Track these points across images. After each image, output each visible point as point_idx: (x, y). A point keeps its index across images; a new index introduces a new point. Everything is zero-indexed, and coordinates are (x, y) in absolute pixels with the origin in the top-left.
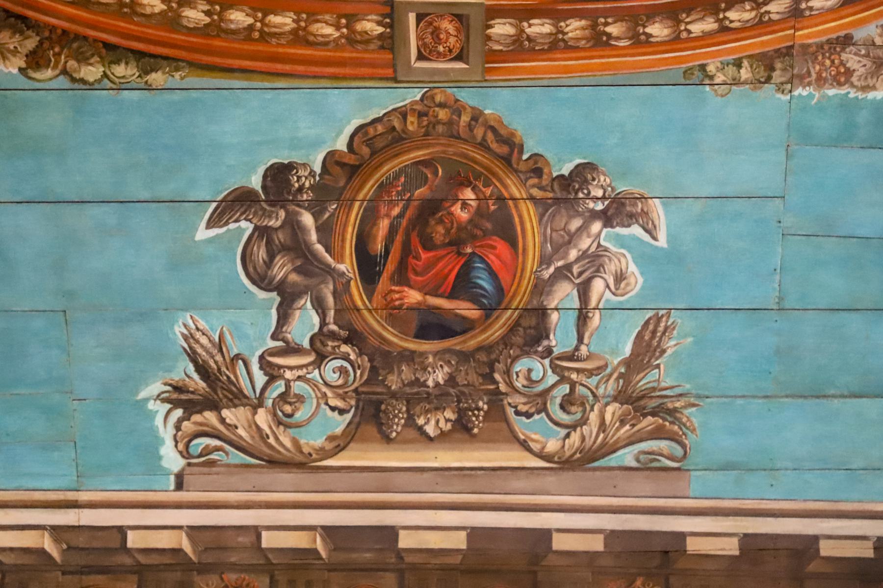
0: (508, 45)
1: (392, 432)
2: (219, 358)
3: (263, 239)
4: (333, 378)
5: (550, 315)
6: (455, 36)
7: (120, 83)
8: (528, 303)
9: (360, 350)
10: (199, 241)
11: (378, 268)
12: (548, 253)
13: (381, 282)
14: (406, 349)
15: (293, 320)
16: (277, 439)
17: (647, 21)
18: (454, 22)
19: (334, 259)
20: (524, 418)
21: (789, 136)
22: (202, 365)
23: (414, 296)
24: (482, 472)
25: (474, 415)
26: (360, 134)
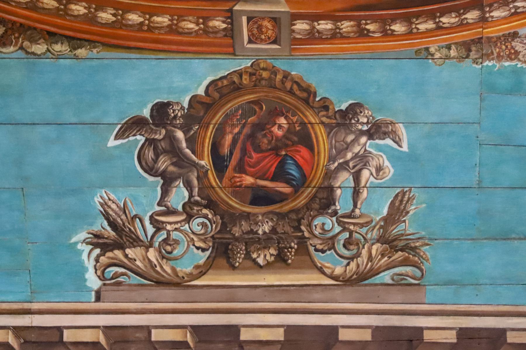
0: (305, 35)
1: (236, 263)
2: (123, 217)
3: (151, 146)
4: (198, 229)
5: (336, 191)
6: (272, 30)
7: (58, 55)
8: (322, 184)
9: (215, 212)
10: (109, 147)
11: (225, 163)
12: (333, 155)
13: (227, 171)
14: (244, 212)
15: (171, 194)
16: (161, 267)
17: (392, 22)
18: (271, 22)
19: (197, 158)
20: (320, 253)
22: (112, 222)
23: (249, 180)
24: (294, 288)
25: (289, 251)
26: (213, 86)
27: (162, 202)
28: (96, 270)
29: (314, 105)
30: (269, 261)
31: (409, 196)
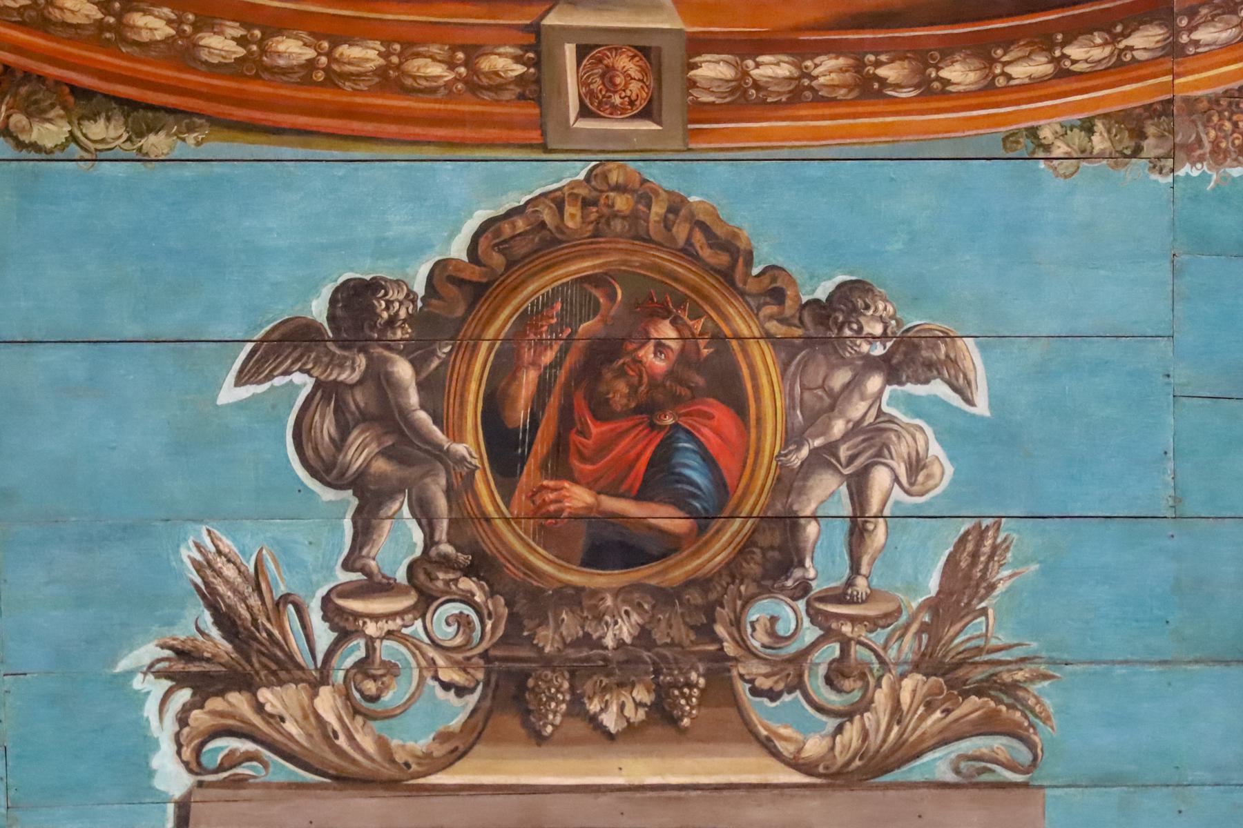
1: (545, 725)
2: (254, 601)
3: (329, 404)
4: (446, 633)
5: (805, 528)
6: (639, 80)
7: (96, 150)
8: (768, 507)
9: (490, 586)
10: (222, 405)
11: (520, 451)
12: (797, 425)
13: (525, 471)
14: (567, 585)
15: (380, 536)
16: (351, 738)
18: (637, 59)
19: (448, 436)
20: (766, 701)
21: (1175, 240)
22: (224, 614)
23: (579, 497)
24: (699, 792)
25: (683, 695)
26: (489, 234)
27: (354, 561)
28: (180, 746)
29: (747, 288)
30: (631, 721)
31: (994, 543)
